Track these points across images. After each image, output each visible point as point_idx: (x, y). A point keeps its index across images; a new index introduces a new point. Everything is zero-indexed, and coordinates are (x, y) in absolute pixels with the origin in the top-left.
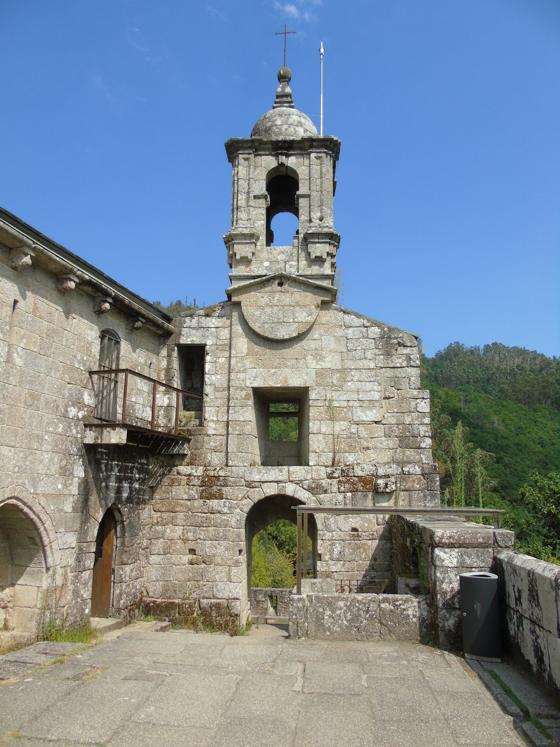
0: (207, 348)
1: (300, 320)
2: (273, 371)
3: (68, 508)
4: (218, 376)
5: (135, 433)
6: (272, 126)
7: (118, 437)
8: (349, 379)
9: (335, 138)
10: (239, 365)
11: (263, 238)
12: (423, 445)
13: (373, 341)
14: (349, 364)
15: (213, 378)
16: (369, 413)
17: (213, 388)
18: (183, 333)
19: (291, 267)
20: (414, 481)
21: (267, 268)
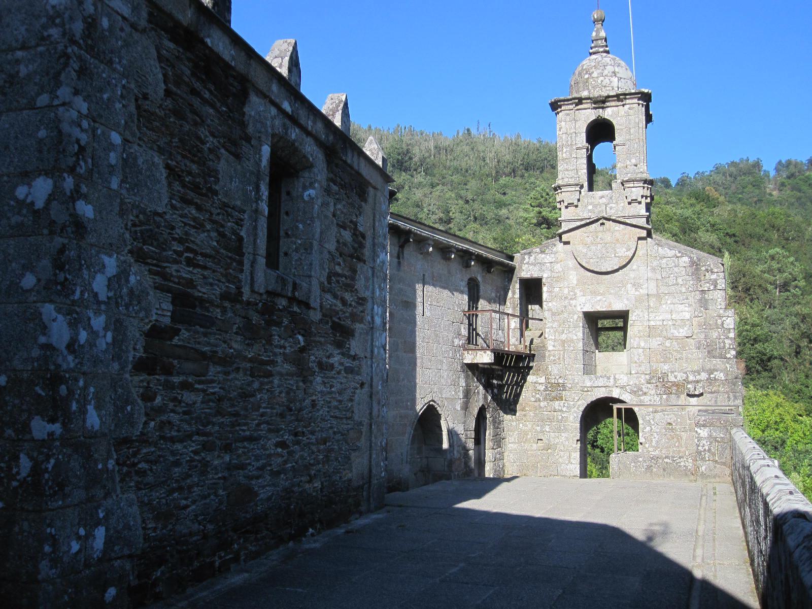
0: (544, 280)
1: (620, 255)
2: (599, 298)
3: (458, 408)
4: (554, 303)
5: (500, 356)
6: (588, 78)
7: (486, 358)
8: (663, 302)
9: (646, 91)
10: (571, 293)
11: (586, 185)
12: (728, 356)
13: (684, 269)
14: (663, 289)
15: (550, 304)
16: (681, 330)
17: (550, 313)
18: (523, 268)
19: (611, 209)
20: (719, 385)
21: (590, 211)
